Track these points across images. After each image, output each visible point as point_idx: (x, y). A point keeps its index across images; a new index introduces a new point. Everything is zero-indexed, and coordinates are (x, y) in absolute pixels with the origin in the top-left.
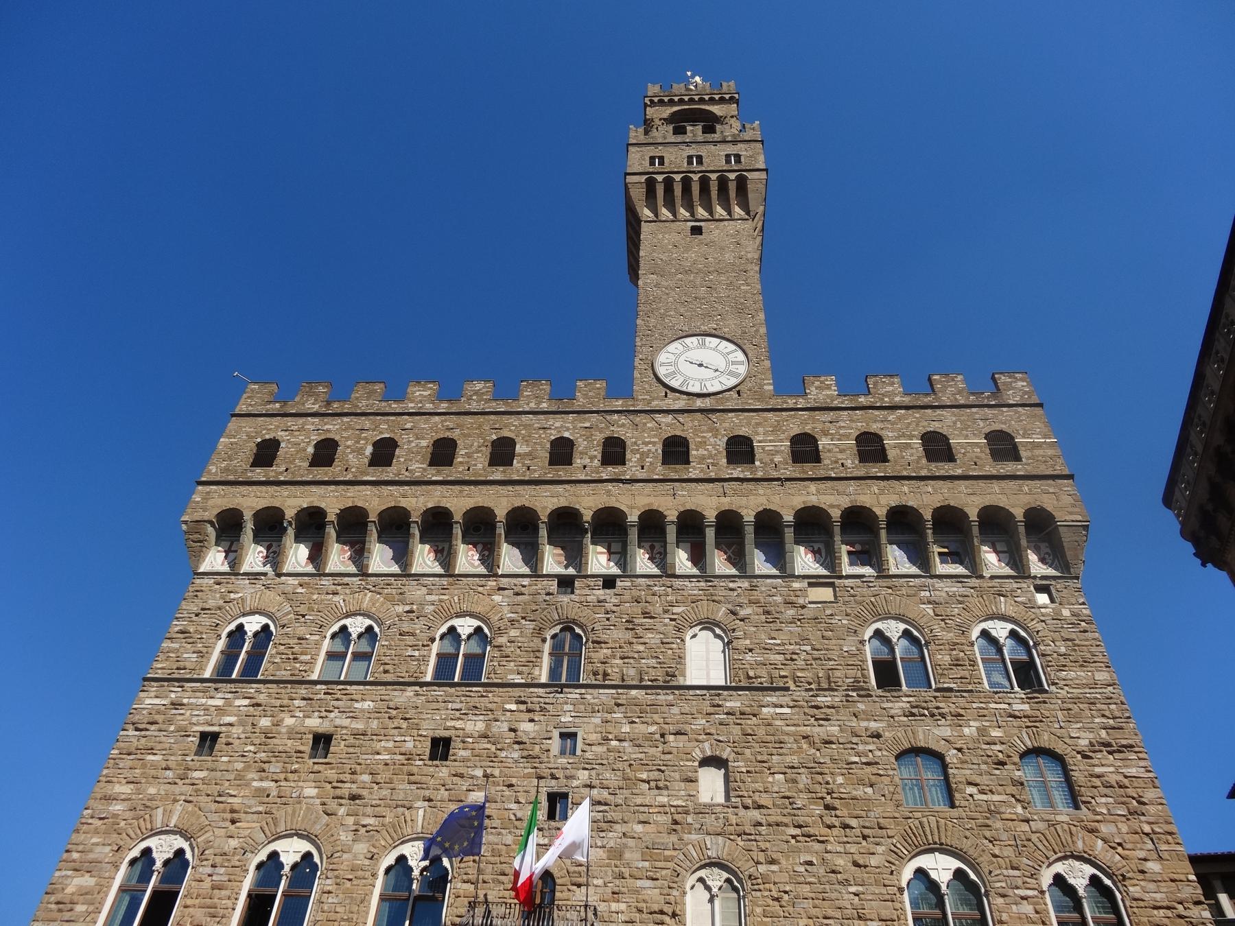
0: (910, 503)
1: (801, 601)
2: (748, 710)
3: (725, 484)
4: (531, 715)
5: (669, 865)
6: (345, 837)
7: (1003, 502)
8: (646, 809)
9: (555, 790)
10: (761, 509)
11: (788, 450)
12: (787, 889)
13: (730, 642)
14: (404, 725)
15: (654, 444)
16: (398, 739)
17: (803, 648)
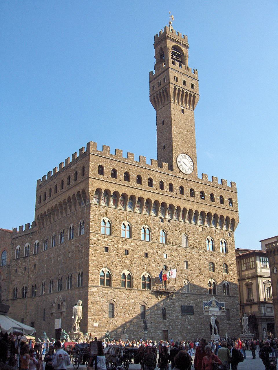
2: (190, 252)
4: (159, 250)
6: (135, 271)
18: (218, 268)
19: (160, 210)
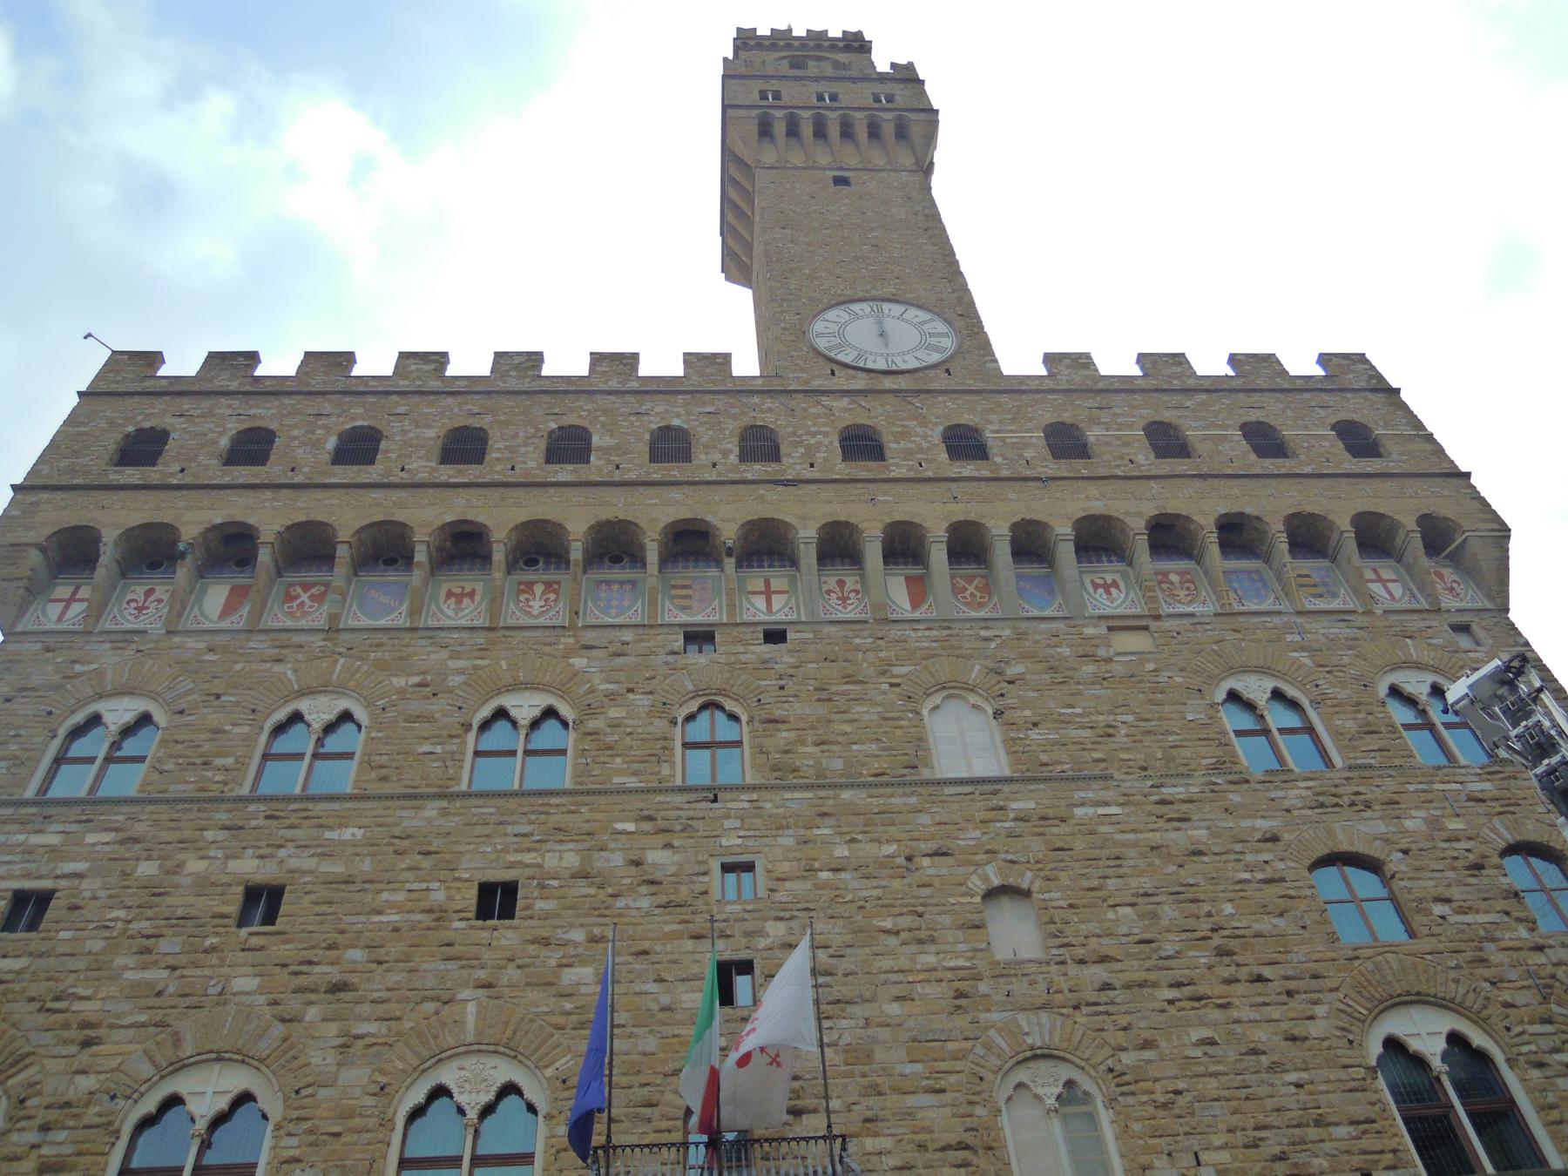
0: (1248, 510)
1: (1102, 652)
2: (1051, 813)
3: (953, 485)
4: (661, 839)
5: (959, 1065)
7: (1382, 508)
8: (901, 977)
9: (727, 956)
10: (1017, 519)
11: (1043, 442)
12: (1180, 1085)
13: (998, 714)
14: (426, 863)
15: (826, 434)
16: (415, 886)
17: (1119, 718)
18: (1442, 891)
19: (685, 587)
